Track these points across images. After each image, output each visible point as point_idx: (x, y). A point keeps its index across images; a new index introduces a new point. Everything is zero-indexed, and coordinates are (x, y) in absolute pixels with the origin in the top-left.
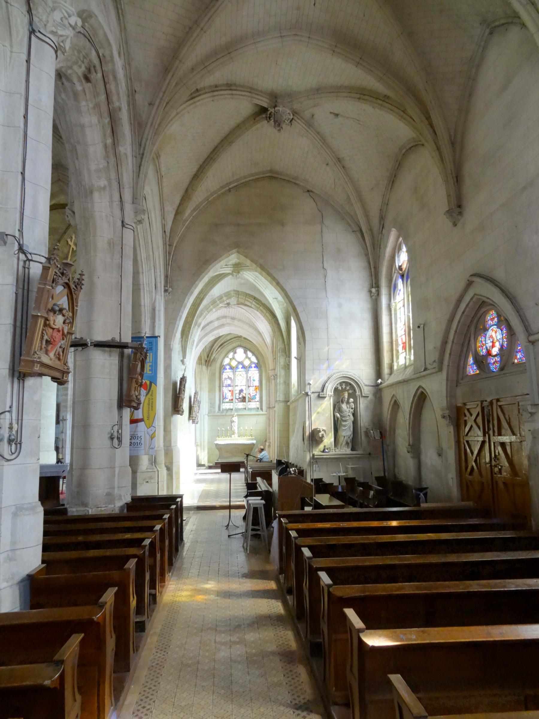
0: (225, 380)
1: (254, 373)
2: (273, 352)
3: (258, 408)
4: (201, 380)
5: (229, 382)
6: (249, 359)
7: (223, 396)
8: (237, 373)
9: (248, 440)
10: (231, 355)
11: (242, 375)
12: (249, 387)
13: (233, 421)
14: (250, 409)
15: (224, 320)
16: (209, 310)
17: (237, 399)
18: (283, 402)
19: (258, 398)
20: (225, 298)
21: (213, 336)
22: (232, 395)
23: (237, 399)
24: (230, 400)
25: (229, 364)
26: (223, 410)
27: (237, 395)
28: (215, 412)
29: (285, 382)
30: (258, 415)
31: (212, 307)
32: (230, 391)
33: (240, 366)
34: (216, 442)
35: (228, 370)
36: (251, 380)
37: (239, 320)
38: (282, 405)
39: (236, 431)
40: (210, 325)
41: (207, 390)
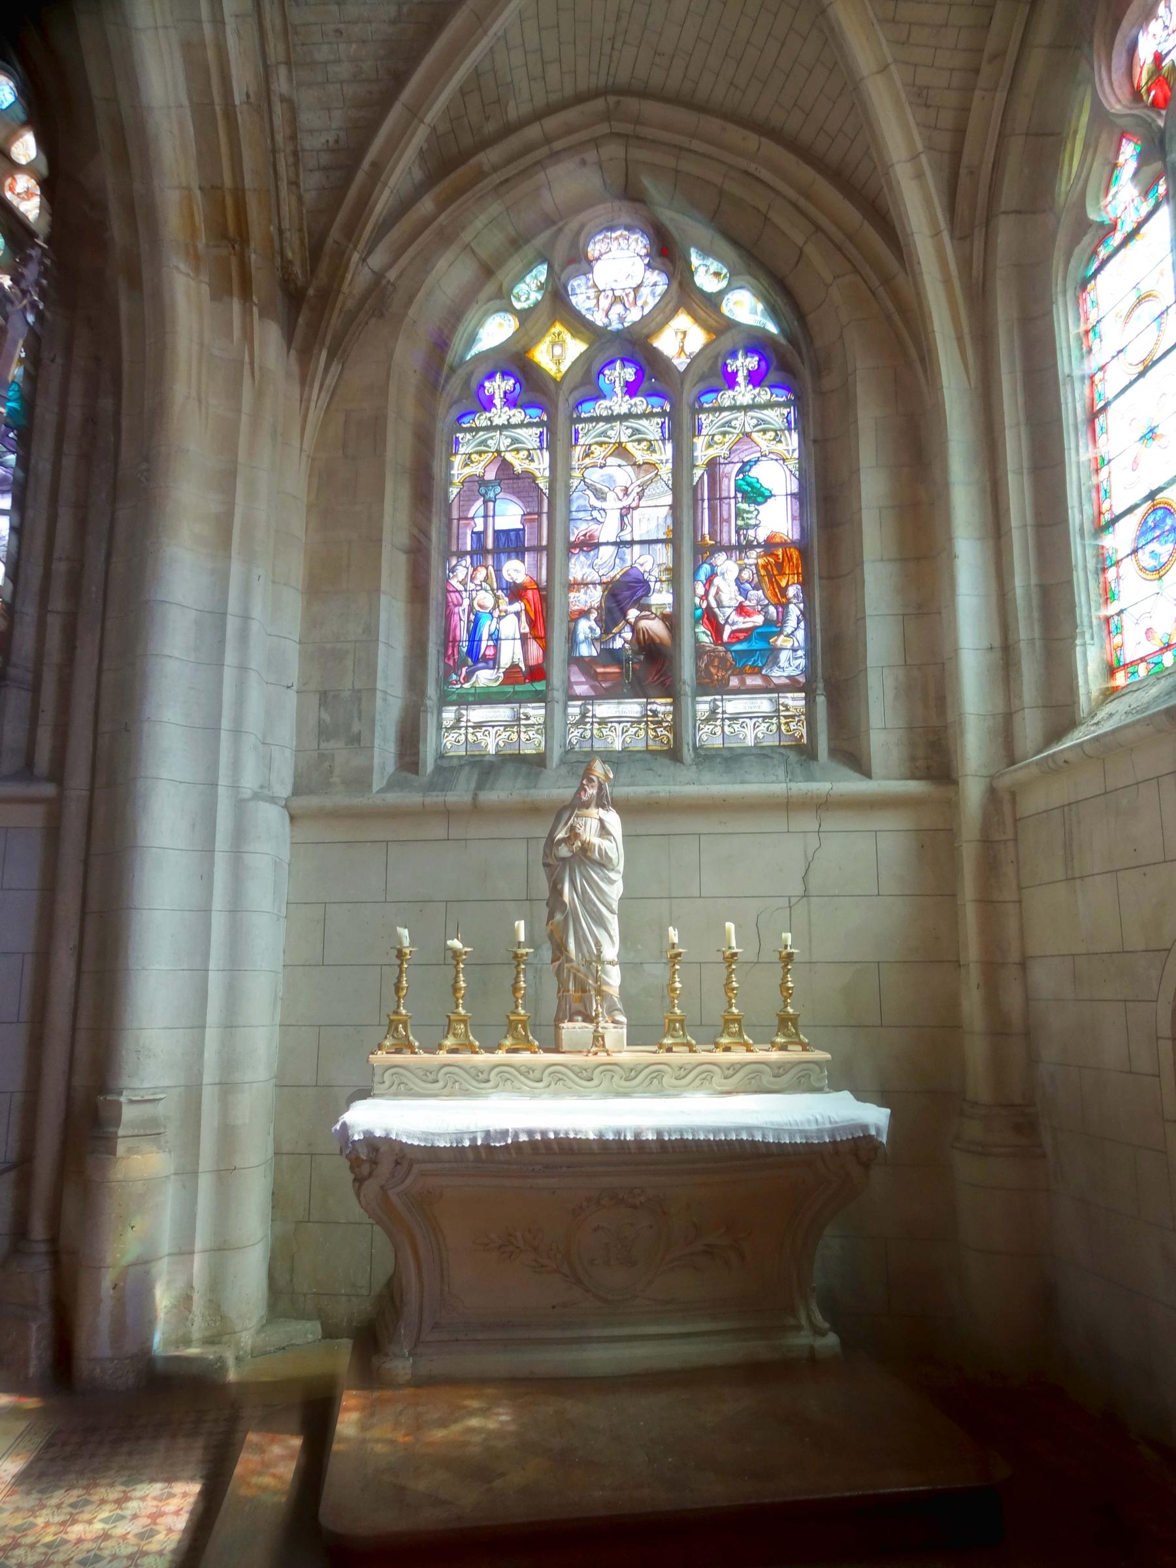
0: (467, 499)
4: (227, 441)
5: (509, 515)
6: (706, 307)
7: (448, 640)
8: (588, 435)
9: (758, 1081)
10: (529, 291)
11: (639, 453)
12: (704, 552)
13: (584, 856)
14: (730, 759)
17: (585, 665)
19: (790, 663)
22: (539, 625)
23: (585, 665)
24: (512, 670)
26: (448, 768)
28: (360, 780)
30: (822, 805)
32: (516, 592)
35: (500, 414)
36: (728, 487)
39: (614, 978)
41: (296, 567)
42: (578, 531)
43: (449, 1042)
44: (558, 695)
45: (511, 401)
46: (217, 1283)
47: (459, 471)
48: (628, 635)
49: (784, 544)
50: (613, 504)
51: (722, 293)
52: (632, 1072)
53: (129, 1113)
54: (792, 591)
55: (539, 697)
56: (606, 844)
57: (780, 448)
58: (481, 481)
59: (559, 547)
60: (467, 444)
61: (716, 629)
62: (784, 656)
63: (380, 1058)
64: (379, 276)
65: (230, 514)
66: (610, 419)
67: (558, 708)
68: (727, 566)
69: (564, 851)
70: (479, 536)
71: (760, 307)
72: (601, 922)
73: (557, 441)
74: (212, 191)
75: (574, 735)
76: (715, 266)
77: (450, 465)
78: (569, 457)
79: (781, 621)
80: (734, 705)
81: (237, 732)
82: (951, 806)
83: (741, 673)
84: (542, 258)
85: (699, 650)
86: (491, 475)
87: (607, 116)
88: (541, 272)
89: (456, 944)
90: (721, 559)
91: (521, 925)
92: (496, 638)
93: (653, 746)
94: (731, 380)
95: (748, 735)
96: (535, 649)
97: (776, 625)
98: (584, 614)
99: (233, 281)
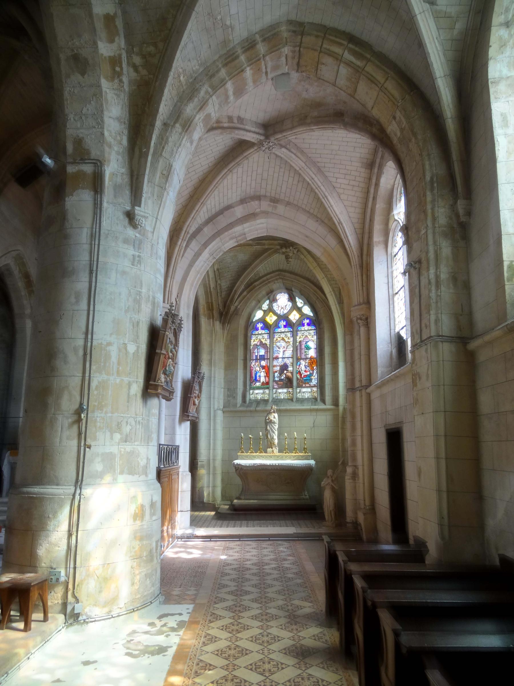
0: (254, 349)
1: (309, 337)
2: (361, 266)
3: (316, 399)
4: (211, 345)
5: (262, 352)
6: (299, 310)
8: (276, 336)
9: (298, 458)
10: (265, 306)
12: (298, 360)
13: (271, 422)
15: (255, 204)
16: (215, 80)
17: (276, 382)
18: (450, 339)
19: (314, 382)
20: (261, 48)
21: (231, 239)
22: (267, 375)
23: (276, 382)
24: (263, 383)
25: (263, 320)
26: (251, 402)
27: (276, 374)
28: (235, 405)
29: (454, 278)
30: (317, 410)
31: (223, 73)
32: (263, 367)
33: (283, 323)
34: (236, 462)
35: (260, 331)
36: (303, 347)
37: (288, 204)
38: (447, 350)
39: (276, 441)
40: (226, 213)
41: (222, 365)
42: (275, 356)
43: (250, 452)
44: (271, 388)
45: (262, 329)
46: (213, 492)
47: (253, 343)
48: (284, 376)
49: (313, 358)
50: (281, 350)
51: (302, 307)
52: (278, 456)
53: (199, 463)
54: (315, 368)
55: (268, 388)
56: (274, 420)
57: (313, 339)
58: (257, 345)
59: (271, 359)
60: (254, 338)
61: (301, 375)
62: (313, 380)
63: (239, 454)
64: (237, 307)
65: (211, 359)
66: (281, 333)
67: (271, 391)
68: (303, 363)
69: (268, 421)
70: (257, 356)
71: (309, 310)
72: (274, 432)
73: (271, 337)
74: (207, 303)
75: (275, 395)
76: (301, 301)
77: (251, 342)
78: (273, 340)
79: (313, 373)
80: (304, 390)
81: (214, 398)
82: (338, 410)
83: (305, 384)
84: (269, 299)
85: (297, 379)
86: (258, 344)
87: (278, 275)
88: (268, 302)
89: (250, 436)
90: (302, 361)
91: (261, 433)
92: (260, 376)
93: (289, 398)
94: (303, 325)
95: (307, 396)
96: (267, 378)
97: (311, 374)
98: (276, 372)
99: (211, 316)
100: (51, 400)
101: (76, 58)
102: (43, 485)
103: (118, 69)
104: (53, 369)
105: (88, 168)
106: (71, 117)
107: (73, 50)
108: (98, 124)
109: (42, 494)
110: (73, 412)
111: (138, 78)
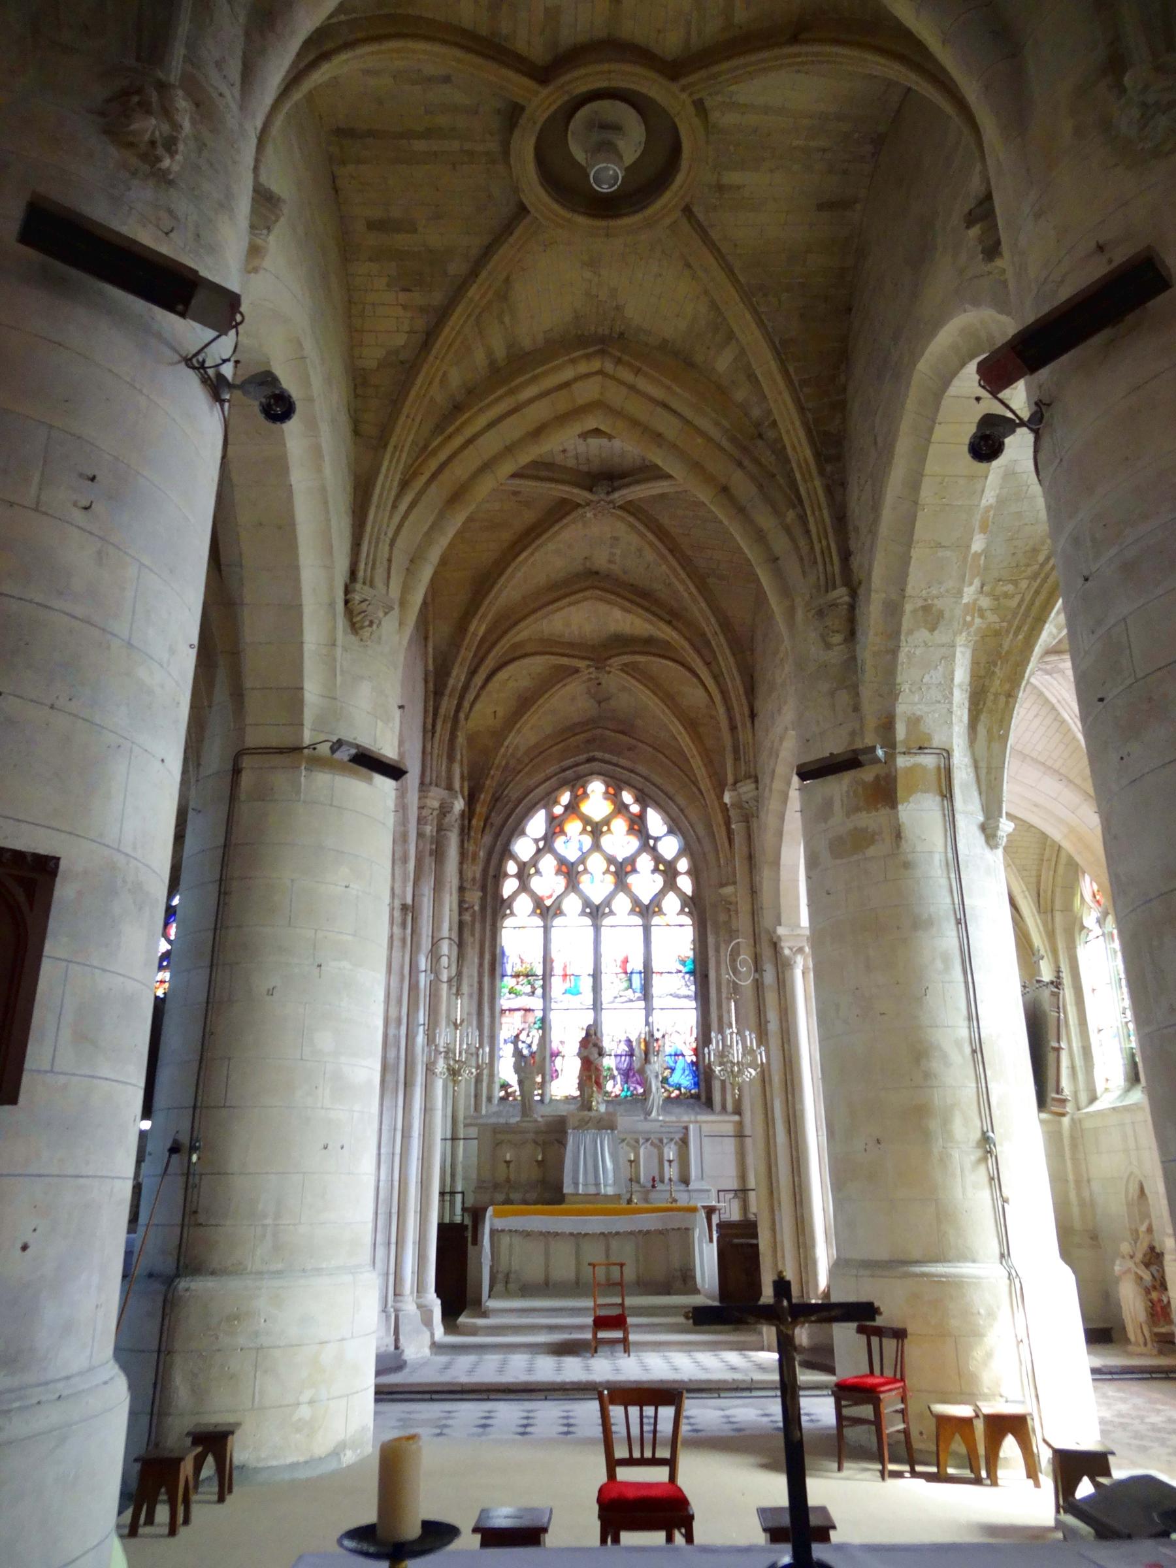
100: (934, 1125)
101: (926, 609)
102: (949, 1261)
103: (969, 618)
104: (927, 1075)
105: (929, 761)
106: (906, 687)
107: (926, 600)
108: (945, 697)
109: (956, 1276)
110: (974, 1144)
111: (984, 626)
